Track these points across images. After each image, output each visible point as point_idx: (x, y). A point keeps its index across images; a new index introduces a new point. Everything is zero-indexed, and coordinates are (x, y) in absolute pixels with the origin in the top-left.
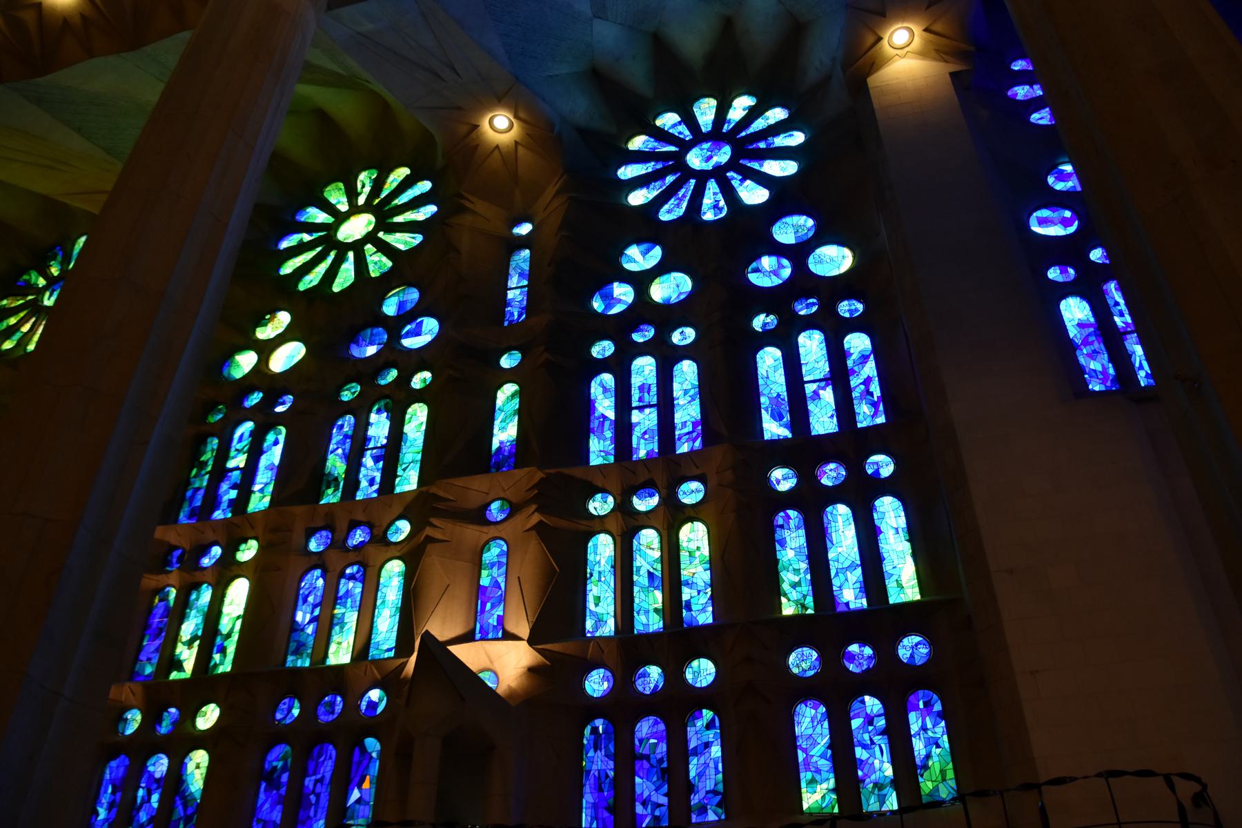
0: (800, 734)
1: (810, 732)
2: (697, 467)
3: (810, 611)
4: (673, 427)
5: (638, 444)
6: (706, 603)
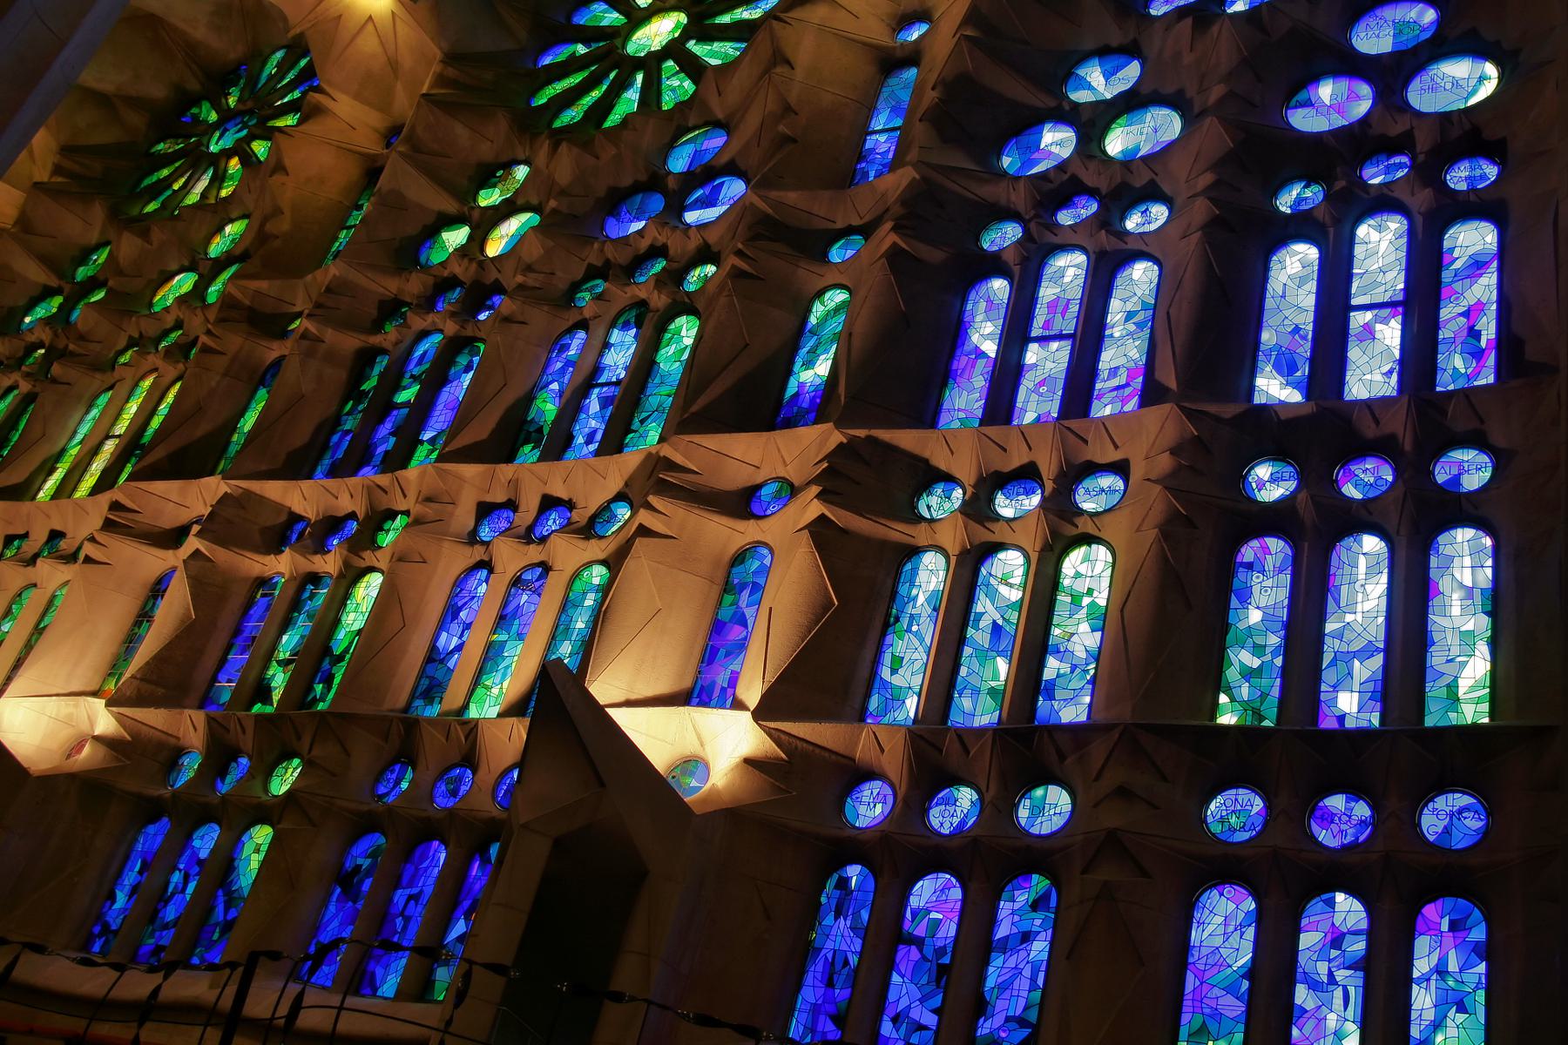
0: (1197, 944)
1: (1218, 941)
2: (1116, 447)
3: (1267, 723)
4: (1093, 374)
5: (1027, 402)
6: (1082, 689)
